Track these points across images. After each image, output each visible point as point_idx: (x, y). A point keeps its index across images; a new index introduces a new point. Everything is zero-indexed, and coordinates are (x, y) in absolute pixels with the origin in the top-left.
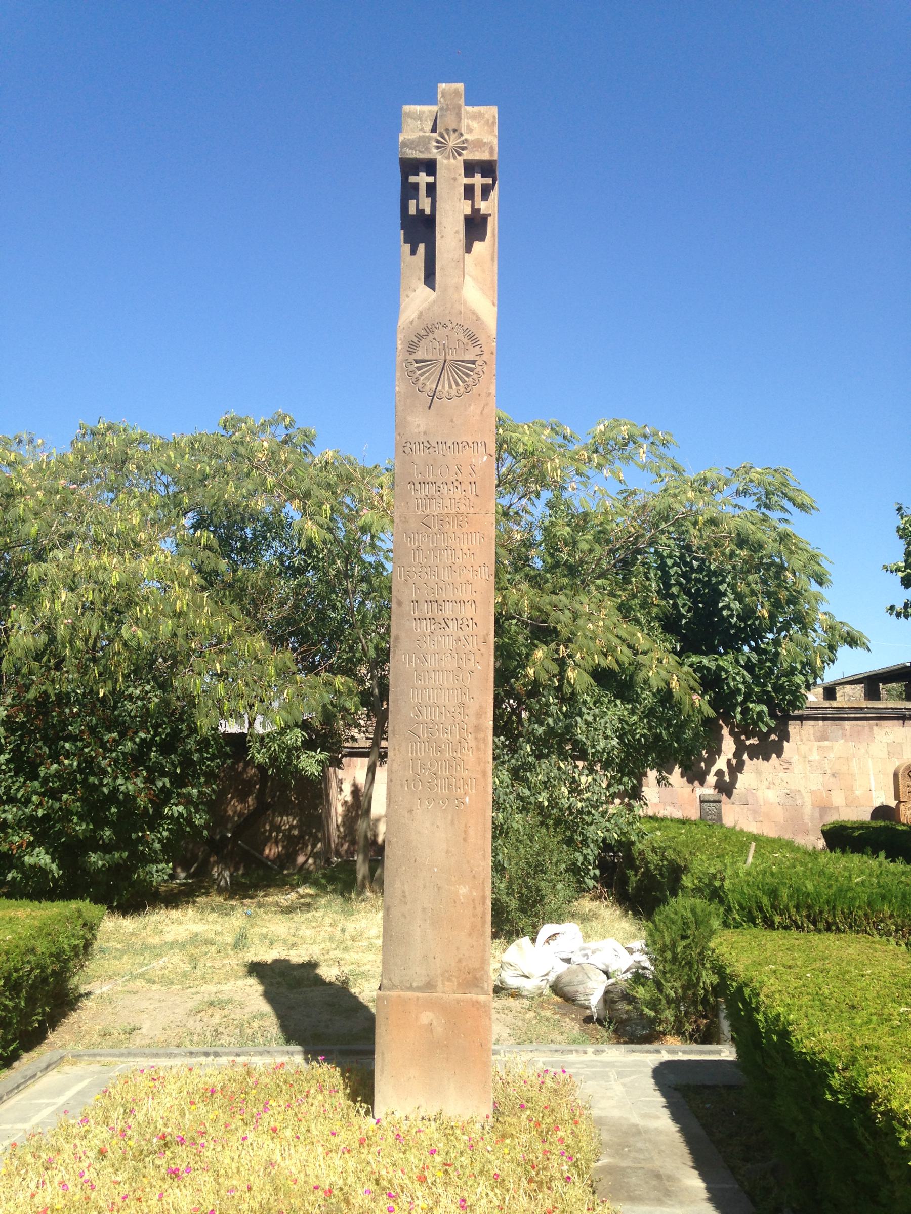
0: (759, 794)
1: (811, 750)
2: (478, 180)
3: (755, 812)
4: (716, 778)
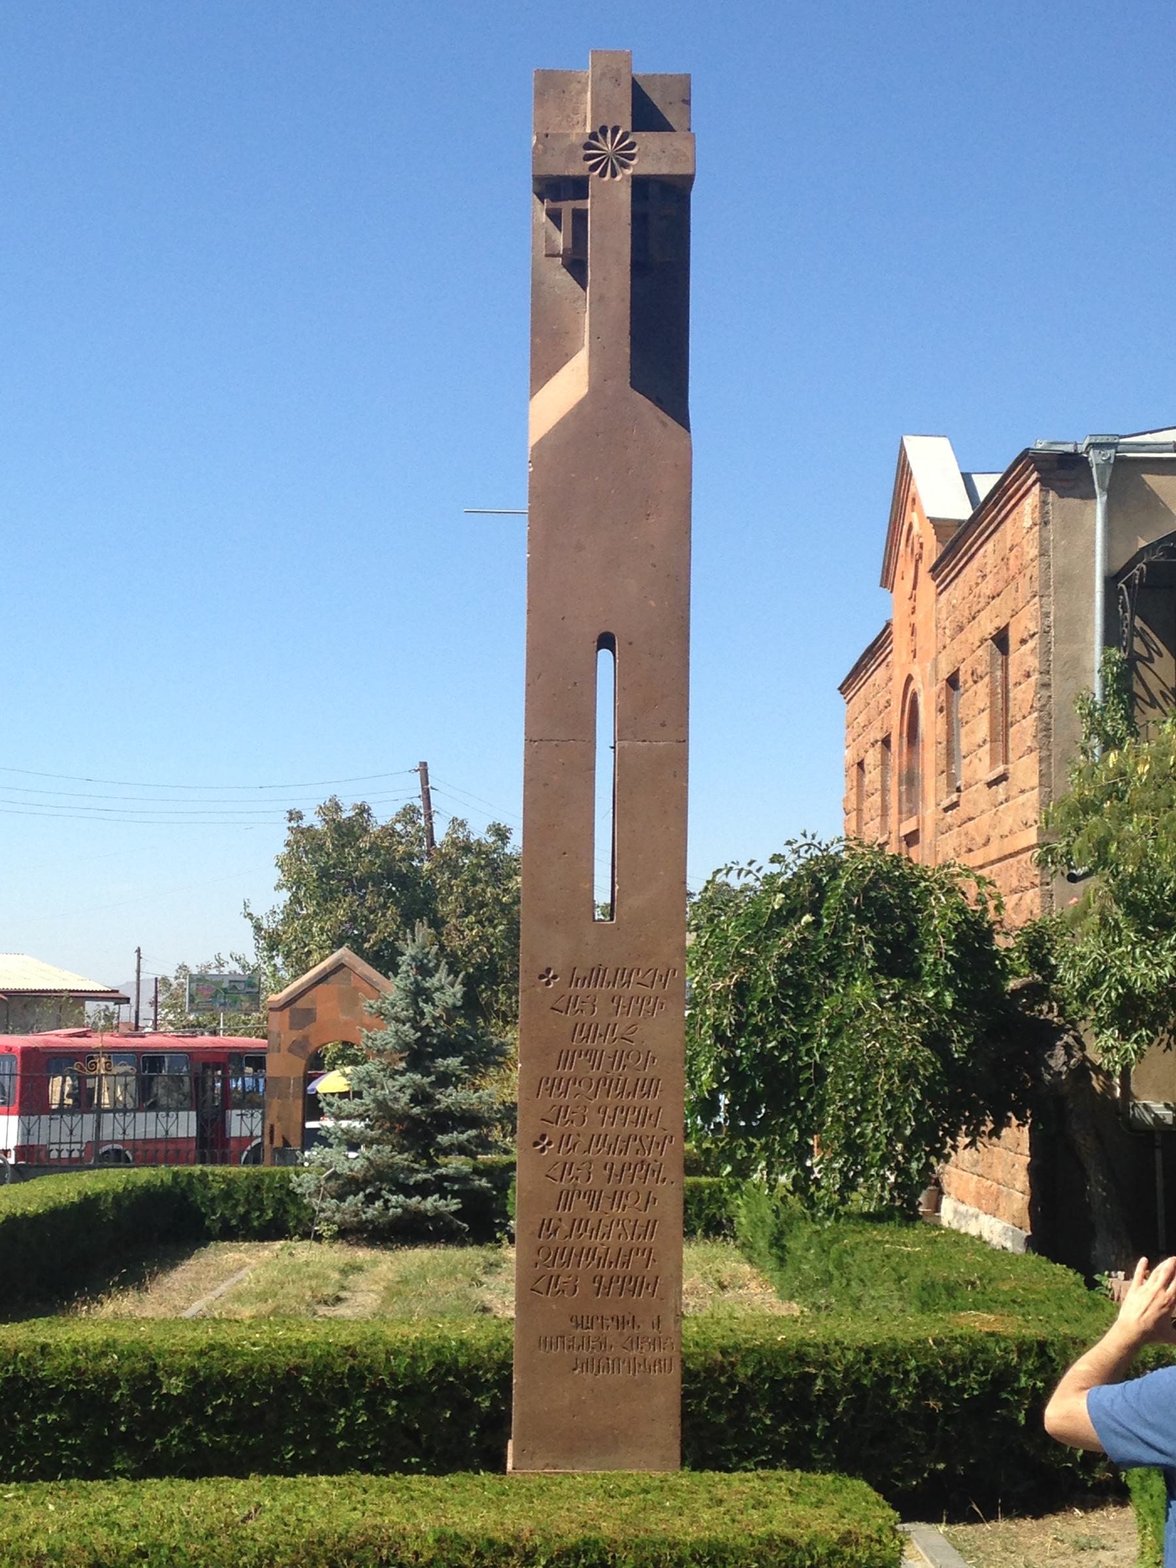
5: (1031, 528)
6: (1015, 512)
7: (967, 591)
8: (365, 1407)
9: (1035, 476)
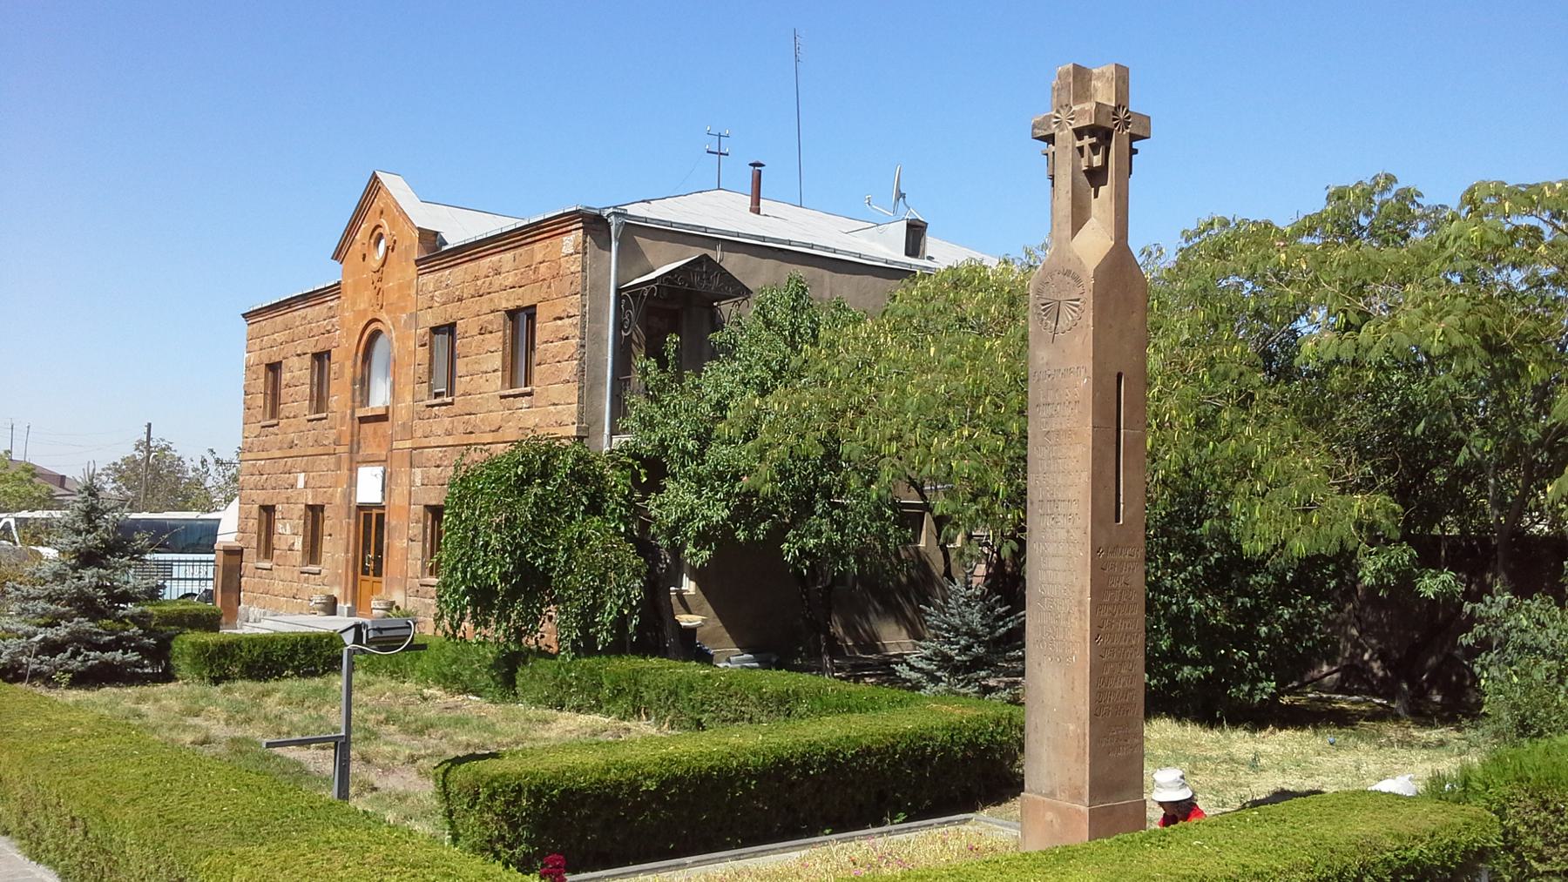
2: (1087, 141)
5: (571, 254)
6: (548, 241)
7: (468, 278)
8: (741, 786)
9: (581, 225)
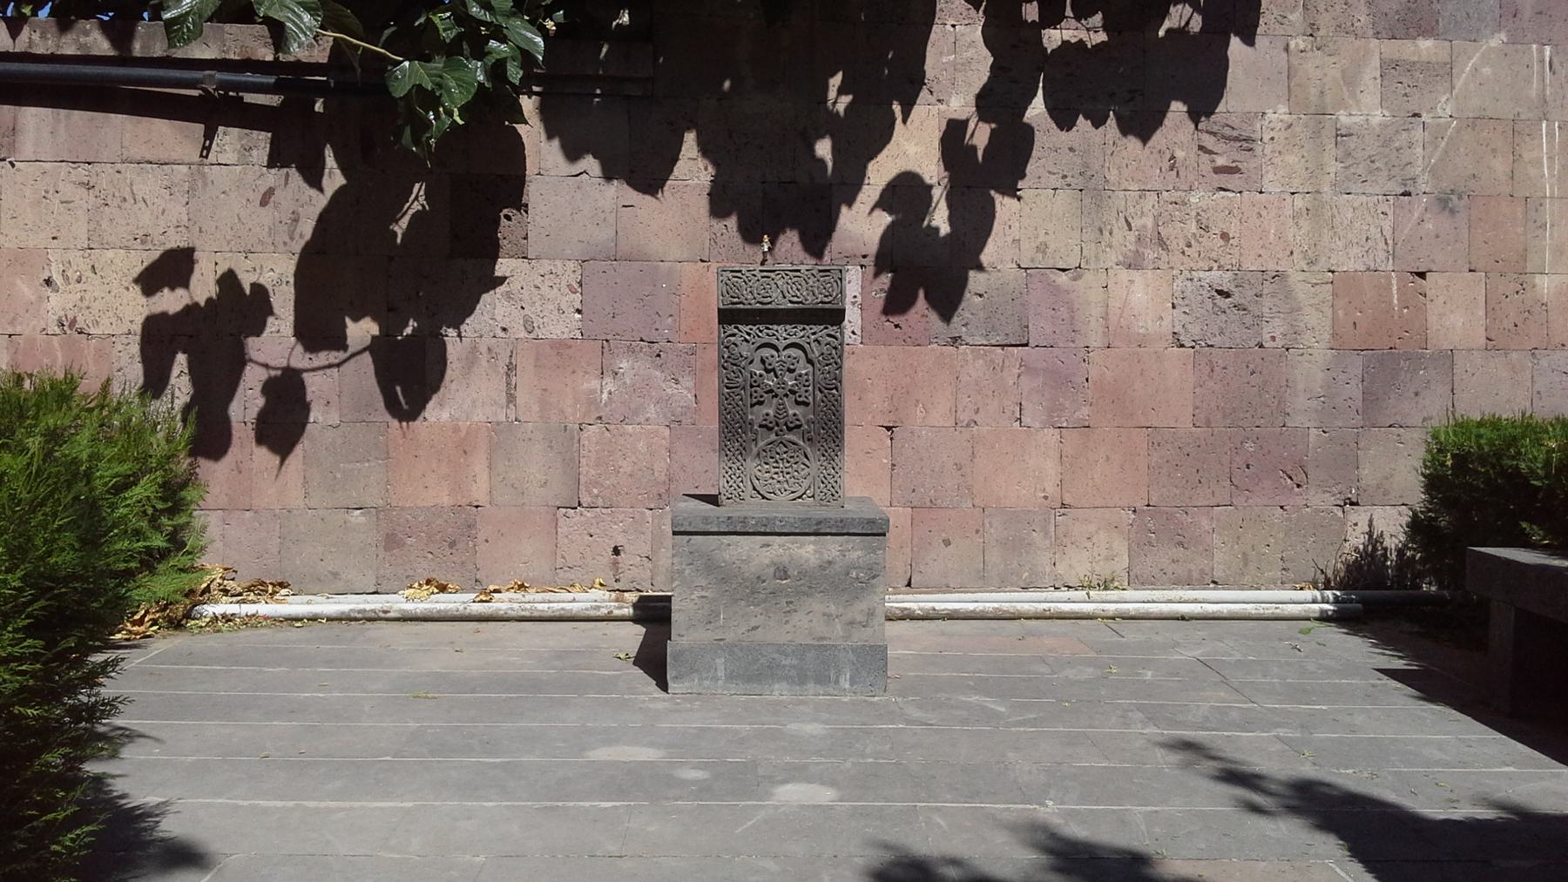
0: (1088, 289)
1: (1350, 80)
3: (1060, 381)
4: (885, 219)
